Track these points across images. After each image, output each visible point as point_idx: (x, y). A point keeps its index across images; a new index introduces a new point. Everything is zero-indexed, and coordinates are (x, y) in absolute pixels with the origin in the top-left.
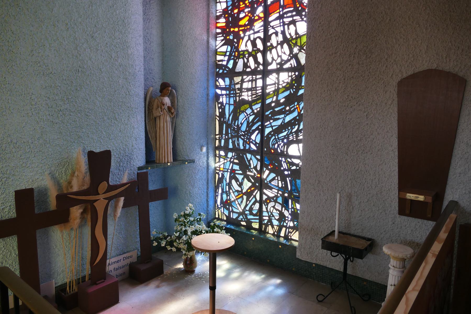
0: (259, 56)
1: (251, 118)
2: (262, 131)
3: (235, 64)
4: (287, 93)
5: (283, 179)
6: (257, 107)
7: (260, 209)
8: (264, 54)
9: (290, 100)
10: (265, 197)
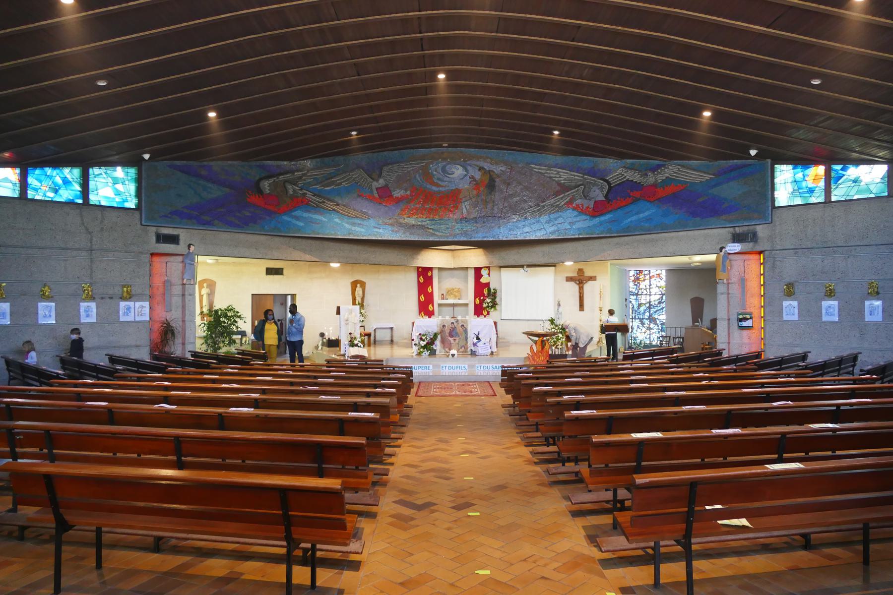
0: (648, 290)
2: (650, 312)
3: (638, 292)
5: (658, 326)
7: (650, 337)
8: (650, 289)
9: (659, 303)
10: (651, 333)
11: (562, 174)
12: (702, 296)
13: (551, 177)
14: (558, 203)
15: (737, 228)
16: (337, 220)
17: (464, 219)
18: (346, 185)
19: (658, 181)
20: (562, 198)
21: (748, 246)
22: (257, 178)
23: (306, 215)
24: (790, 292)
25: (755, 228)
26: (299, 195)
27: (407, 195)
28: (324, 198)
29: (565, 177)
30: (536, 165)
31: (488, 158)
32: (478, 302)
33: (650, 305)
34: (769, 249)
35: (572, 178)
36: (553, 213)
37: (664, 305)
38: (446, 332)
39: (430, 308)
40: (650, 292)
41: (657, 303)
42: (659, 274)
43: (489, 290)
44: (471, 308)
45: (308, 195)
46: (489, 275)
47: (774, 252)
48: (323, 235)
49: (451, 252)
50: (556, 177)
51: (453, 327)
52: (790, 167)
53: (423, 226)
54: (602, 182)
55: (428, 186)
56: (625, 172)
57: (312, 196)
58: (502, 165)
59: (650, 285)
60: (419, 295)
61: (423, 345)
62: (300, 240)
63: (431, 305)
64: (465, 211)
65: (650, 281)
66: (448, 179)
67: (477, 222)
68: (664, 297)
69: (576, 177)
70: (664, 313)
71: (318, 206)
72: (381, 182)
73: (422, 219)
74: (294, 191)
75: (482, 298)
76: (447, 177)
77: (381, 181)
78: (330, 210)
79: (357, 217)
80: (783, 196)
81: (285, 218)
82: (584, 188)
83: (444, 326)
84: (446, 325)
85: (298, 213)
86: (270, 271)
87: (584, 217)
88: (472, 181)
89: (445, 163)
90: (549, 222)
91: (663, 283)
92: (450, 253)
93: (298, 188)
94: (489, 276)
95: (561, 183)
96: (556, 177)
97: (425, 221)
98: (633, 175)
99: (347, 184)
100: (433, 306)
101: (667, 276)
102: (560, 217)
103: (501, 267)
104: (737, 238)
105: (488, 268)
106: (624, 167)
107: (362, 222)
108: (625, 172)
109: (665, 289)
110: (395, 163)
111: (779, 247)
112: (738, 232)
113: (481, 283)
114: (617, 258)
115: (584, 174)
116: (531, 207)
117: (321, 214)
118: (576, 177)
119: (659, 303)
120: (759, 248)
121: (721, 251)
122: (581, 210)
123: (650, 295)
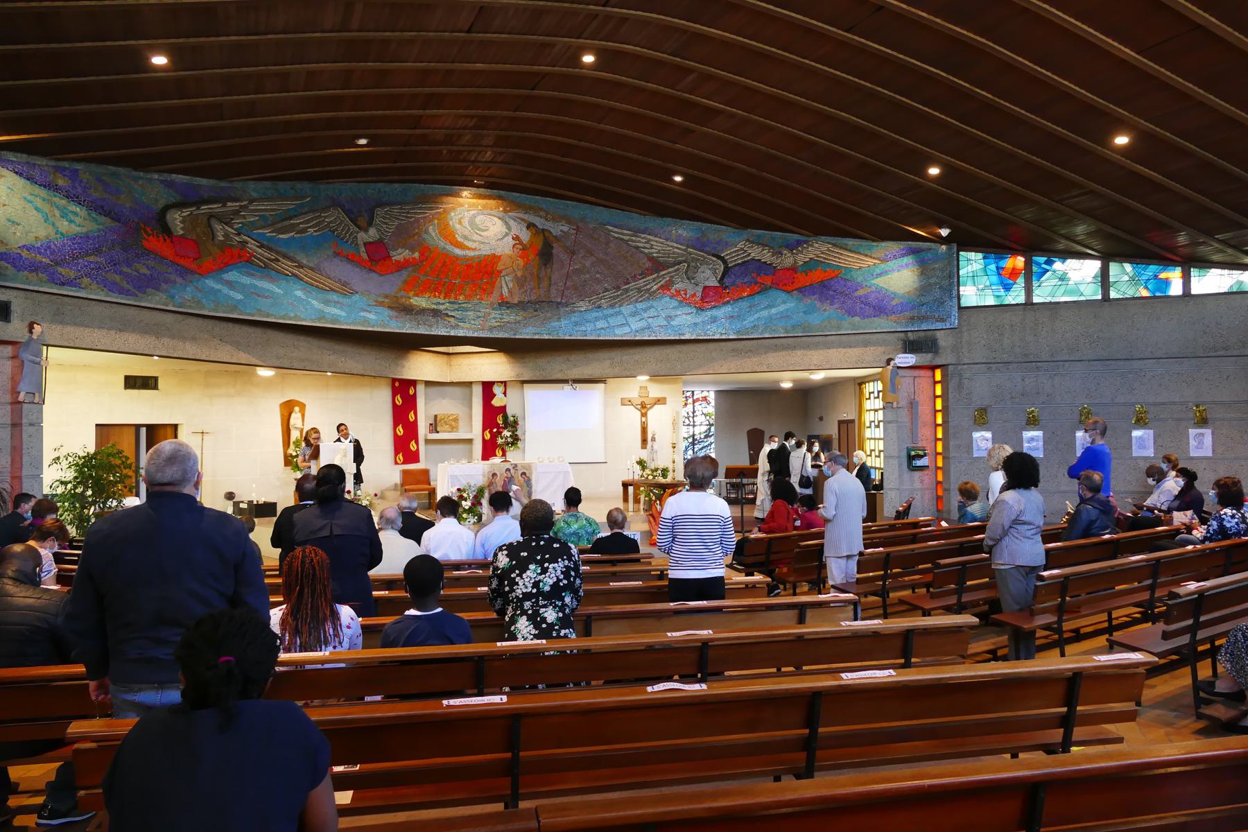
0: (691, 419)
1: (687, 445)
2: (693, 450)
4: (705, 434)
6: (690, 440)
8: (693, 417)
9: (706, 437)
11: (654, 243)
12: (761, 427)
13: (637, 248)
14: (648, 287)
15: (910, 334)
16: (299, 293)
17: (504, 304)
18: (314, 234)
19: (798, 263)
20: (654, 280)
21: (926, 359)
22: (162, 203)
23: (246, 280)
24: (981, 419)
25: (935, 334)
26: (236, 243)
27: (414, 259)
28: (277, 253)
29: (659, 248)
30: (615, 227)
31: (541, 209)
32: (488, 436)
33: (694, 440)
34: (954, 363)
35: (670, 250)
36: (641, 301)
37: (712, 439)
38: (498, 484)
39: (413, 446)
40: (694, 422)
41: (702, 436)
42: (705, 397)
43: (505, 417)
44: (478, 447)
45: (249, 245)
46: (505, 394)
47: (960, 367)
48: (276, 318)
49: (446, 356)
50: (645, 248)
51: (509, 476)
52: (980, 255)
53: (440, 311)
54: (714, 259)
55: (447, 247)
56: (748, 248)
57: (258, 247)
58: (564, 223)
59: (694, 412)
60: (395, 426)
61: (467, 508)
62: (230, 325)
63: (413, 442)
64: (506, 290)
65: (694, 406)
66: (479, 238)
67: (524, 310)
68: (713, 429)
69: (676, 250)
70: (712, 450)
71: (266, 266)
72: (372, 234)
73: (439, 300)
74: (226, 235)
75: (495, 430)
76: (477, 234)
77: (372, 231)
78: (288, 275)
79: (332, 290)
80: (970, 295)
81: (210, 283)
82: (688, 266)
83: (494, 475)
84: (498, 474)
85: (232, 275)
86: (132, 382)
87: (687, 310)
88: (516, 244)
89: (474, 212)
90: (634, 314)
91: (711, 409)
92: (445, 358)
93: (233, 231)
94: (505, 396)
95: (653, 257)
96: (645, 248)
97: (443, 304)
98: (761, 252)
99: (315, 231)
100: (417, 443)
101: (716, 399)
102: (652, 307)
103: (524, 382)
104: (911, 346)
105: (505, 383)
106: (748, 240)
107: (341, 300)
108: (748, 248)
109: (713, 417)
110: (394, 204)
111: (966, 361)
112: (911, 338)
113: (492, 406)
114: (733, 371)
115: (688, 246)
116: (607, 290)
117: (273, 280)
118: (676, 250)
119: (706, 437)
120: (939, 361)
121: (889, 364)
122: (685, 301)
123: (694, 426)
